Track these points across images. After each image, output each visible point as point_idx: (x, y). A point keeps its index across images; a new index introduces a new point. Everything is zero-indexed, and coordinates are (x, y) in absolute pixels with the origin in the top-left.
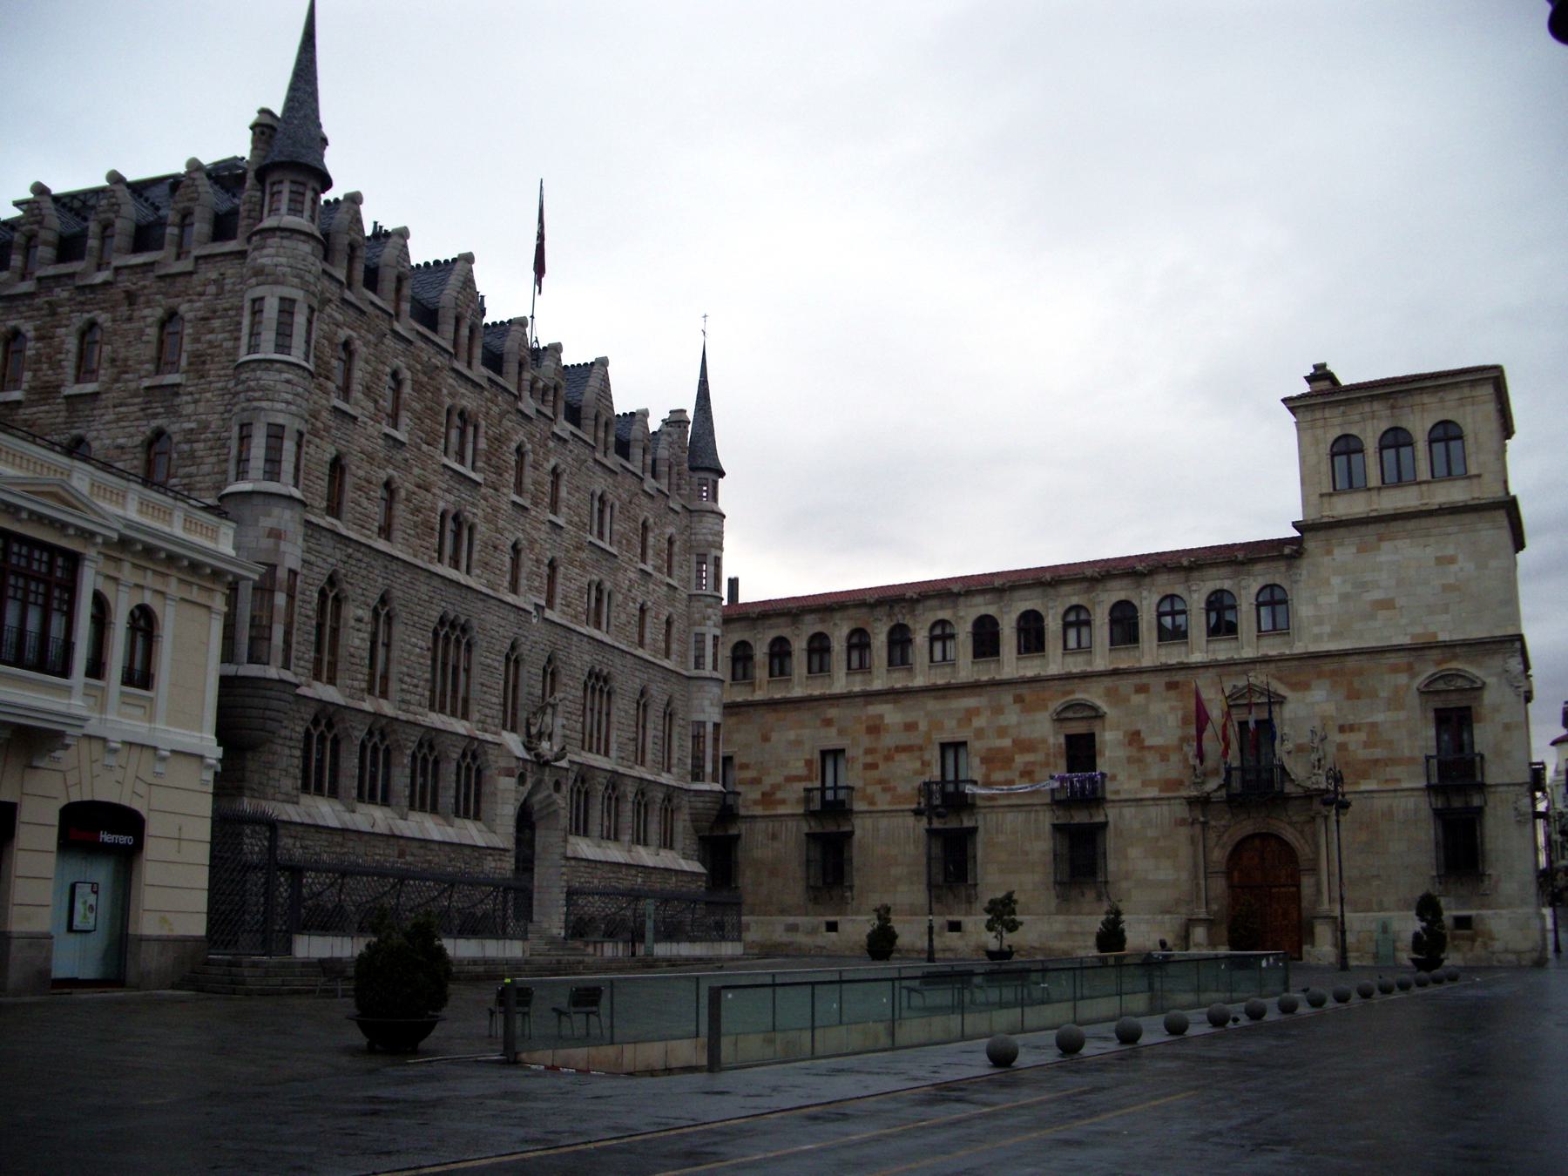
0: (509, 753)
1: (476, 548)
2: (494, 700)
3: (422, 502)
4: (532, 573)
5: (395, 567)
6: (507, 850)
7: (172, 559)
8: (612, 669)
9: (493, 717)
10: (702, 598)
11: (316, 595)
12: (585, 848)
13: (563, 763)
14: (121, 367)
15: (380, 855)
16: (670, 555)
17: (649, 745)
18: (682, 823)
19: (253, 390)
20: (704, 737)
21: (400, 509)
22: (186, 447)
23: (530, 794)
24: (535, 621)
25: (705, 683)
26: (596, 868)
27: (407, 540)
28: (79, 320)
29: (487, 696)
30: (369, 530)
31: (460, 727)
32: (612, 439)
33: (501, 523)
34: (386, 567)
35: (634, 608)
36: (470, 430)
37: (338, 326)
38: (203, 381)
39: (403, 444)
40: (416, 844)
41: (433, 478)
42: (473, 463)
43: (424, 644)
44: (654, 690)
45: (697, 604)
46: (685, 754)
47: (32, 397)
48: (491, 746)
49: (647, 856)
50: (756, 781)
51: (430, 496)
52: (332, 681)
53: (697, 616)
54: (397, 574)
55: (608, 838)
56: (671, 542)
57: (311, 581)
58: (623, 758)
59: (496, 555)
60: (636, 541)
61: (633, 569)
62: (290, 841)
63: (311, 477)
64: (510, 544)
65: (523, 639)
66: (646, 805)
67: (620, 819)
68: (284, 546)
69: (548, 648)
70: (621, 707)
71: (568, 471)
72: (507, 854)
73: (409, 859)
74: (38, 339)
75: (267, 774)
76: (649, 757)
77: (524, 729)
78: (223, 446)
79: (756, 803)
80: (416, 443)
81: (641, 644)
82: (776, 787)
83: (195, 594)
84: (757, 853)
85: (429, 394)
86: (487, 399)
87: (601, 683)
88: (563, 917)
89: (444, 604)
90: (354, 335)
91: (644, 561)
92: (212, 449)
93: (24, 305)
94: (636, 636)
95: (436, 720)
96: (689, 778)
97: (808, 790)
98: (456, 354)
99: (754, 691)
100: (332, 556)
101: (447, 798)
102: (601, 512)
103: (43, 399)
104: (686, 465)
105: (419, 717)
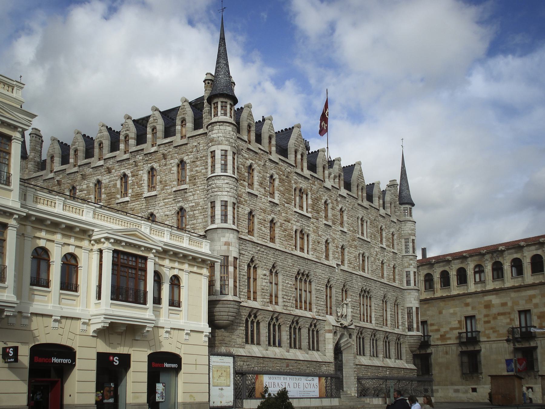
0: (330, 324)
1: (311, 243)
2: (322, 303)
4: (334, 251)
5: (277, 253)
6: (332, 363)
7: (185, 256)
8: (371, 288)
11: (246, 267)
12: (365, 360)
13: (352, 327)
14: (165, 184)
16: (393, 240)
17: (389, 318)
18: (405, 349)
19: (214, 188)
20: (412, 313)
21: (277, 230)
22: (191, 213)
23: (340, 339)
24: (337, 271)
25: (411, 291)
27: (282, 242)
28: (147, 167)
29: (319, 302)
30: (266, 239)
32: (365, 195)
33: (320, 233)
34: (274, 254)
35: (379, 263)
36: (304, 196)
37: (246, 159)
38: (195, 186)
39: (277, 204)
41: (291, 217)
42: (307, 210)
43: (291, 283)
44: (389, 295)
45: (405, 259)
47: (133, 199)
48: (322, 321)
49: (391, 363)
50: (438, 330)
51: (290, 224)
54: (279, 256)
55: (374, 356)
56: (393, 235)
58: (377, 324)
59: (319, 245)
60: (378, 235)
61: (378, 247)
62: (242, 363)
64: (324, 241)
65: (333, 278)
66: (389, 342)
67: (378, 348)
68: (231, 248)
69: (343, 281)
70: (376, 303)
71: (347, 210)
72: (331, 364)
74: (133, 176)
76: (389, 323)
77: (335, 314)
78: (206, 211)
79: (438, 339)
80: (283, 203)
81: (383, 277)
82: (446, 332)
84: (440, 360)
85: (286, 183)
86: (311, 183)
87: (367, 294)
88: (356, 389)
89: (299, 267)
90: (254, 162)
91: (382, 243)
92: (201, 213)
93: (126, 163)
94: (380, 274)
95: (298, 312)
97: (460, 333)
98: (296, 166)
99: (434, 294)
100: (250, 251)
101: (305, 343)
102: (362, 225)
103: (136, 199)
104: (398, 203)
105: (291, 312)
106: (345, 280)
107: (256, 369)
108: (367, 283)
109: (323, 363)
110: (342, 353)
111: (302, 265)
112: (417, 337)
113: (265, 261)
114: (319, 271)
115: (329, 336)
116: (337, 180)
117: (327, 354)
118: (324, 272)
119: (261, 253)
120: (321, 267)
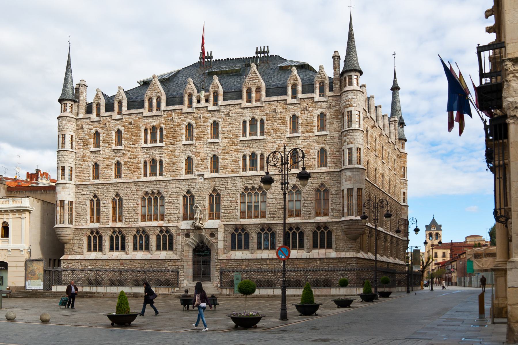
1: (164, 166)
3: (133, 162)
9: (175, 218)
21: (124, 168)
26: (243, 262)
29: (170, 212)
31: (154, 224)
33: (177, 154)
57: (84, 199)
58: (273, 217)
65: (191, 189)
70: (271, 197)
73: (125, 265)
85: (133, 130)
89: (145, 189)
107: (89, 267)
110: (210, 251)
114: (172, 187)
116: (211, 98)
117: (178, 253)
118: (179, 186)
119: (101, 189)
120: (175, 183)
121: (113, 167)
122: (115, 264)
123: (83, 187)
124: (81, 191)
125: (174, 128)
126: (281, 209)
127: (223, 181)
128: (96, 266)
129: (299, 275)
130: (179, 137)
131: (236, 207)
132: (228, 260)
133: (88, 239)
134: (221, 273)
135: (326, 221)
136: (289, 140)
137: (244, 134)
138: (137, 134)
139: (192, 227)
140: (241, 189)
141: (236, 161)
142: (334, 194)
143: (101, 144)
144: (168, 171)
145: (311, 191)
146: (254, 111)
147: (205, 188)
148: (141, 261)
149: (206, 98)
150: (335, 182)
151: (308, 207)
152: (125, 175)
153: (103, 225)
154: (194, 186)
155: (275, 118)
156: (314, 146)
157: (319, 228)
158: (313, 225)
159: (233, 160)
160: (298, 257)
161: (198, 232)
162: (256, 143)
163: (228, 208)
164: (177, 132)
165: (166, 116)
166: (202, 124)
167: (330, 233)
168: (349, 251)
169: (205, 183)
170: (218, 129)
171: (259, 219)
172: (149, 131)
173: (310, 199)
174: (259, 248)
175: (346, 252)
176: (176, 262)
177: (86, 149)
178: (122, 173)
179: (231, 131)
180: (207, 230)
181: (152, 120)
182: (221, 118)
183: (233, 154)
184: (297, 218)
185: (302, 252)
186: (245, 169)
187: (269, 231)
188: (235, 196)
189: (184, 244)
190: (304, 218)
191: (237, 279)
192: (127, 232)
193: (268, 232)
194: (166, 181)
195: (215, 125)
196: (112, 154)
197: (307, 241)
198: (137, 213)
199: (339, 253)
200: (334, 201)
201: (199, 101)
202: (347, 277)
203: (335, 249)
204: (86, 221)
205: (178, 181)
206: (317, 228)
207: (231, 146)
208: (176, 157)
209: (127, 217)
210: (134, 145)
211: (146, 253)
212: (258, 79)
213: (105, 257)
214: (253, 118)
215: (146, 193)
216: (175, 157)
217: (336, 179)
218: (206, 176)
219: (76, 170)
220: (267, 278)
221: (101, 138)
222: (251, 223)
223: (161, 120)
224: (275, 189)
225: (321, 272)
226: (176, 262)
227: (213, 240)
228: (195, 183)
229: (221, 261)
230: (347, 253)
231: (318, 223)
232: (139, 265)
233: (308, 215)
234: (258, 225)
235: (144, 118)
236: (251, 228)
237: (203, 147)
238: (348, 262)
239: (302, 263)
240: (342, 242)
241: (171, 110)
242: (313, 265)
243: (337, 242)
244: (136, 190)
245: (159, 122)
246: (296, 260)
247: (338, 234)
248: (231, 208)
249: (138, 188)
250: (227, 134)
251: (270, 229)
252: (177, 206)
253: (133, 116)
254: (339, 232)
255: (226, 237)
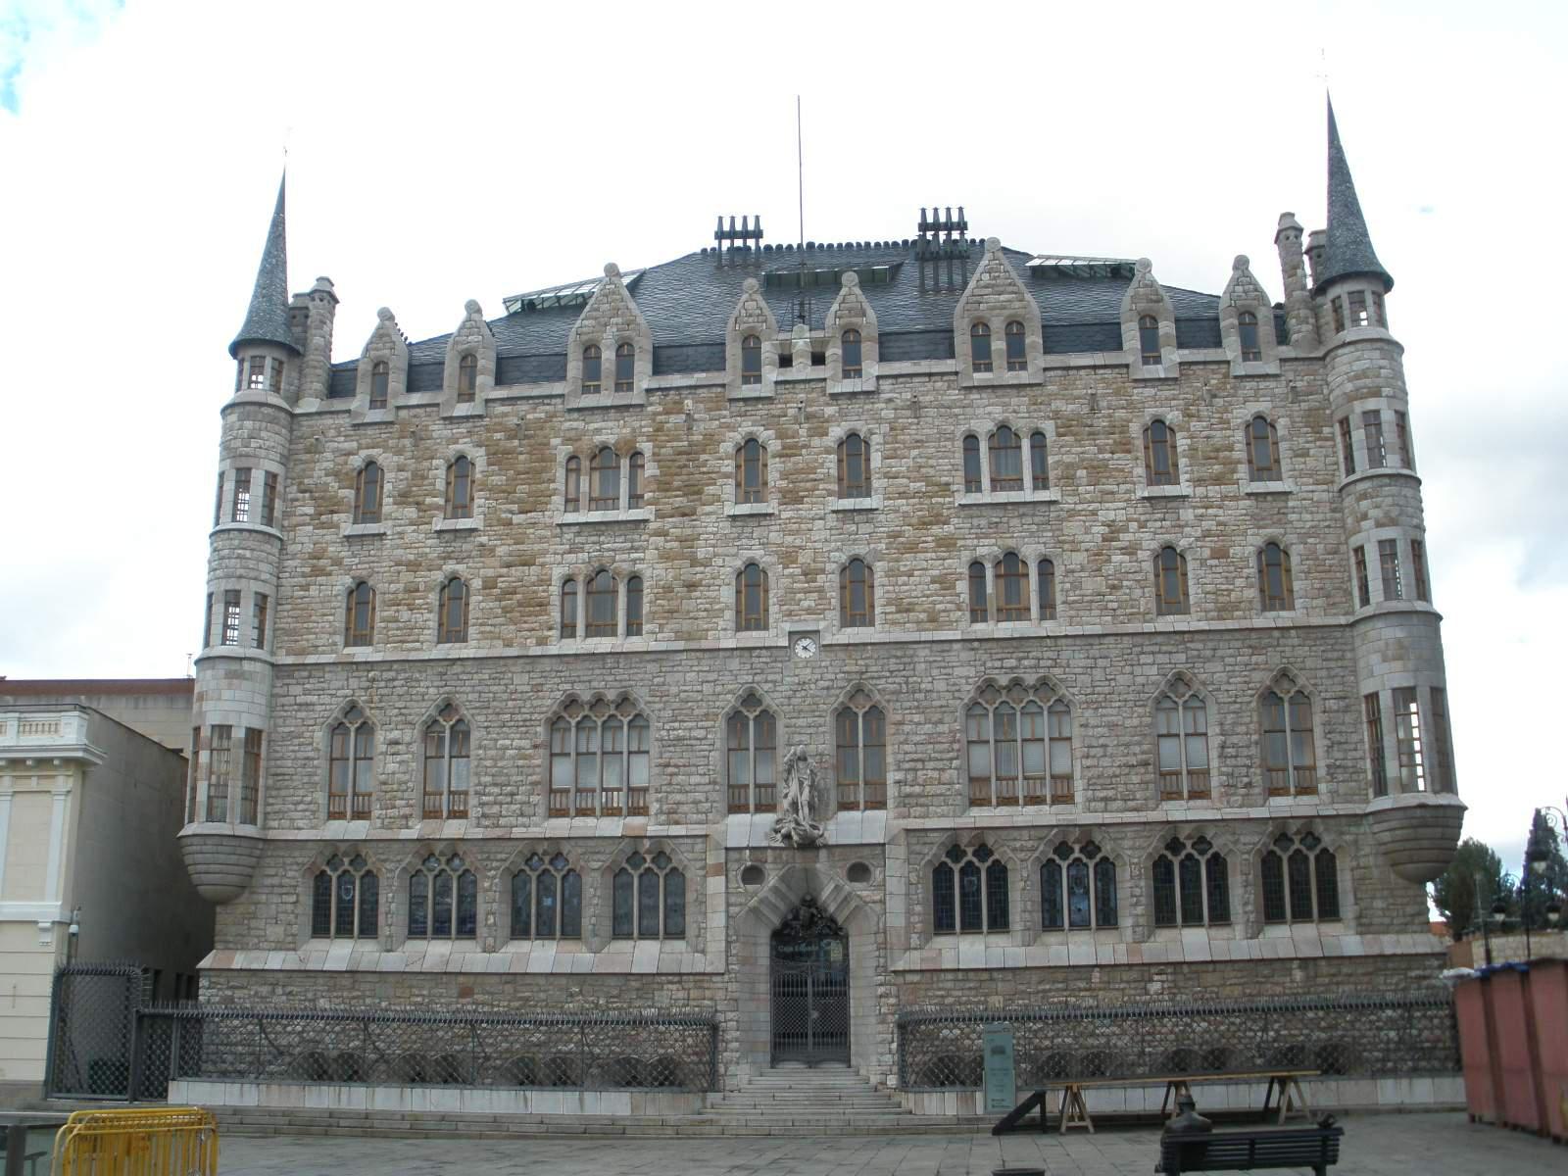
9: (696, 802)
10: (1352, 487)
15: (423, 996)
21: (478, 603)
26: (991, 979)
27: (491, 632)
29: (675, 780)
31: (612, 827)
33: (701, 554)
40: (496, 979)
45: (1349, 501)
46: (1359, 754)
52: (361, 815)
53: (1349, 521)
57: (312, 722)
58: (1105, 799)
59: (698, 594)
63: (313, 618)
65: (766, 687)
70: (1092, 722)
73: (479, 997)
75: (248, 925)
76: (1215, 781)
83: (33, 784)
85: (521, 457)
86: (656, 414)
89: (568, 686)
95: (559, 827)
96: (1371, 791)
106: (854, 676)
107: (322, 1003)
108: (1020, 659)
109: (663, 978)
111: (582, 679)
112: (1400, 814)
113: (397, 705)
114: (686, 679)
115: (716, 884)
116: (834, 351)
117: (712, 947)
118: (714, 676)
119: (383, 684)
121: (433, 598)
122: (435, 991)
123: (305, 674)
124: (296, 690)
125: (692, 452)
126: (1133, 766)
127: (897, 657)
128: (354, 998)
129: (1222, 1028)
130: (711, 490)
131: (952, 759)
132: (928, 975)
133: (317, 888)
134: (902, 1027)
135: (1314, 813)
136: (1150, 510)
137: (972, 483)
138: (538, 472)
139: (773, 839)
140: (969, 687)
141: (945, 583)
142: (1337, 711)
143: (386, 509)
144: (664, 618)
145: (1247, 699)
146: (1006, 400)
147: (822, 684)
148: (551, 979)
149: (818, 350)
150: (1332, 664)
151: (1241, 761)
152: (488, 628)
153: (389, 828)
154: (778, 677)
155: (1091, 426)
156: (1244, 534)
157: (1282, 838)
158: (1264, 828)
159: (932, 577)
160: (1215, 958)
161: (799, 860)
162: (1024, 515)
163: (919, 765)
164: (705, 469)
165: (660, 409)
166: (803, 440)
167: (1327, 861)
168: (1410, 928)
169: (823, 664)
170: (868, 460)
171: (1047, 807)
172: (585, 464)
173: (1243, 729)
174: (1051, 921)
175: (1398, 932)
176: (706, 985)
177: (322, 526)
178: (471, 622)
179: (923, 470)
180: (837, 851)
181: (603, 424)
182: (879, 420)
183: (933, 555)
184: (1199, 802)
185: (1226, 936)
186: (978, 613)
187: (1091, 856)
188: (947, 718)
189: (737, 909)
190: (1228, 802)
191: (999, 1051)
192: (488, 859)
193: (1085, 860)
194: (659, 656)
195: (853, 446)
196: (432, 548)
197: (1246, 892)
198: (535, 784)
199: (1369, 937)
200: (1337, 737)
201: (785, 361)
202: (1415, 1032)
203: (1353, 924)
204: (314, 812)
205: (707, 655)
206: (1275, 843)
207: (924, 523)
208: (702, 565)
209: (491, 798)
210: (523, 516)
211: (570, 946)
212: (1015, 289)
213: (392, 961)
214: (1003, 427)
215: (571, 702)
216: (694, 562)
217: (1335, 655)
218: (827, 640)
219: (279, 608)
220: (1093, 1047)
221: (388, 487)
222: (1020, 821)
223: (637, 424)
224: (1107, 690)
225: (1310, 1015)
226: (706, 985)
227: (865, 893)
228: (780, 665)
229: (900, 980)
230: (1403, 938)
231: (1281, 822)
232: (542, 995)
233: (1243, 791)
234: (1045, 831)
235: (567, 416)
236: (1018, 844)
237: (810, 526)
238: (1413, 974)
239: (1233, 981)
240: (1378, 894)
241: (678, 388)
242: (1278, 989)
243: (1359, 896)
244: (528, 688)
245: (628, 430)
246: (1211, 967)
247: (1363, 862)
248: (931, 765)
249: (539, 681)
250: (905, 481)
251: (1091, 848)
252: (707, 753)
253: (523, 407)
254: (1365, 856)
255: (913, 878)
